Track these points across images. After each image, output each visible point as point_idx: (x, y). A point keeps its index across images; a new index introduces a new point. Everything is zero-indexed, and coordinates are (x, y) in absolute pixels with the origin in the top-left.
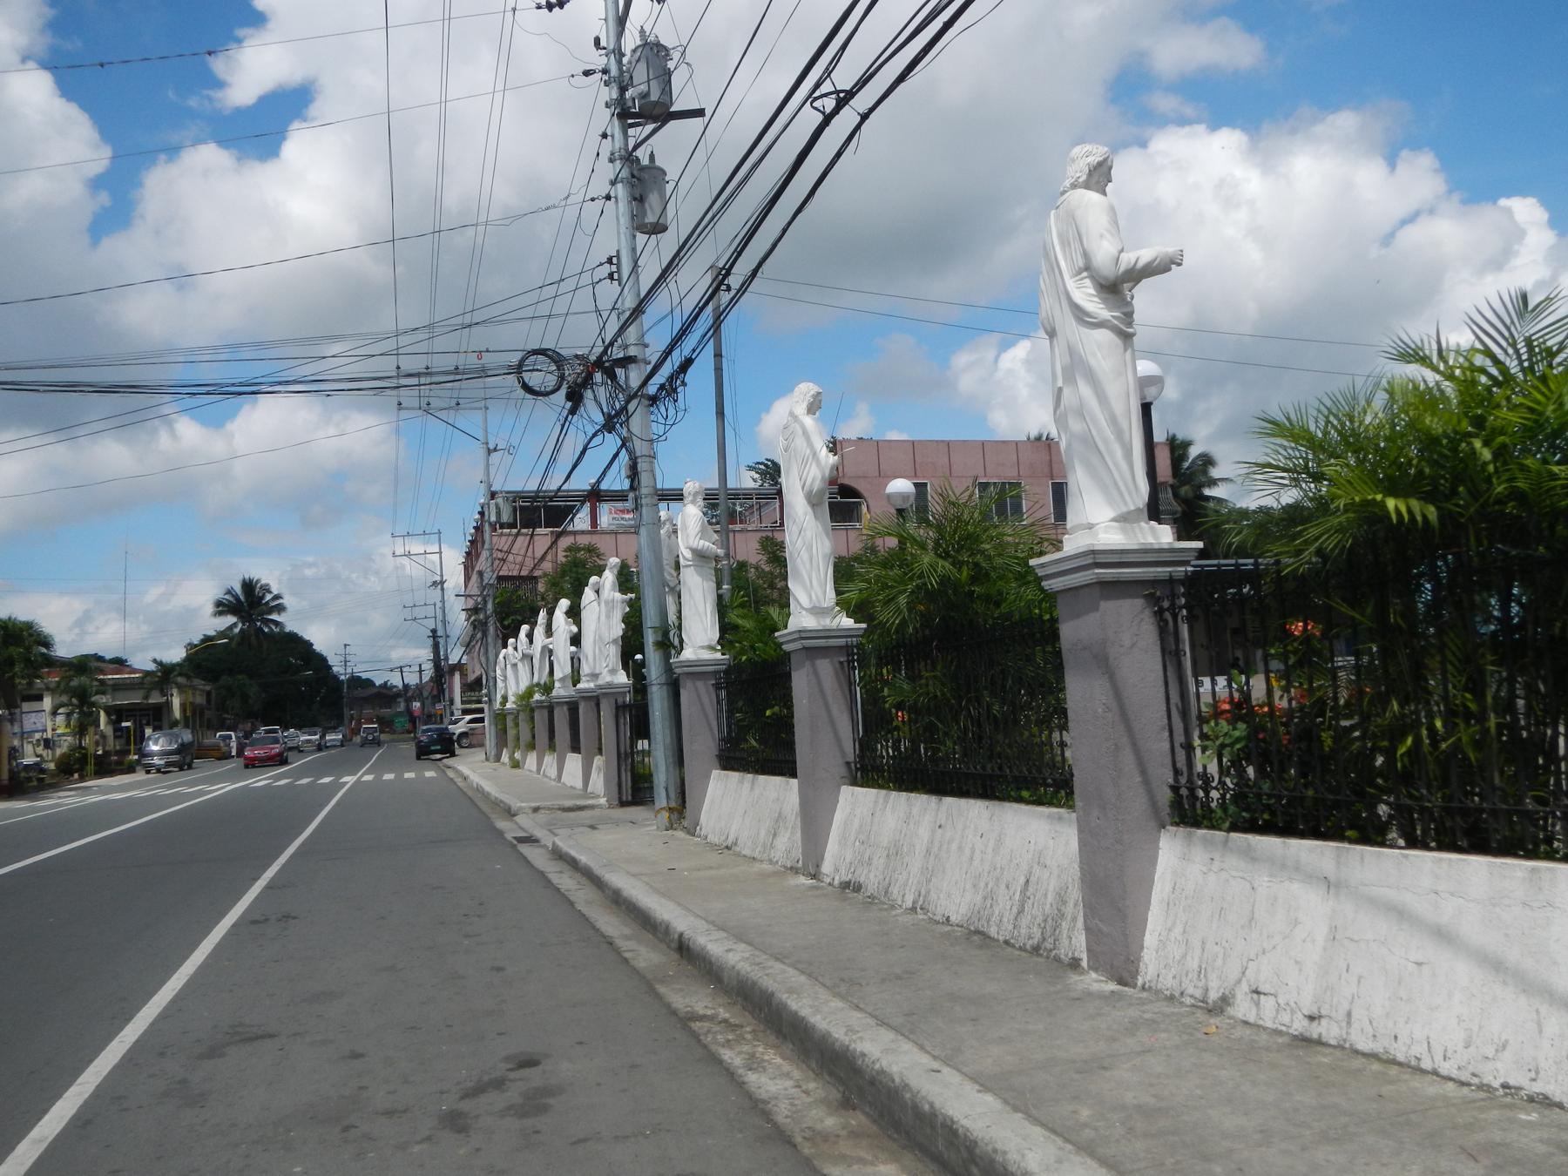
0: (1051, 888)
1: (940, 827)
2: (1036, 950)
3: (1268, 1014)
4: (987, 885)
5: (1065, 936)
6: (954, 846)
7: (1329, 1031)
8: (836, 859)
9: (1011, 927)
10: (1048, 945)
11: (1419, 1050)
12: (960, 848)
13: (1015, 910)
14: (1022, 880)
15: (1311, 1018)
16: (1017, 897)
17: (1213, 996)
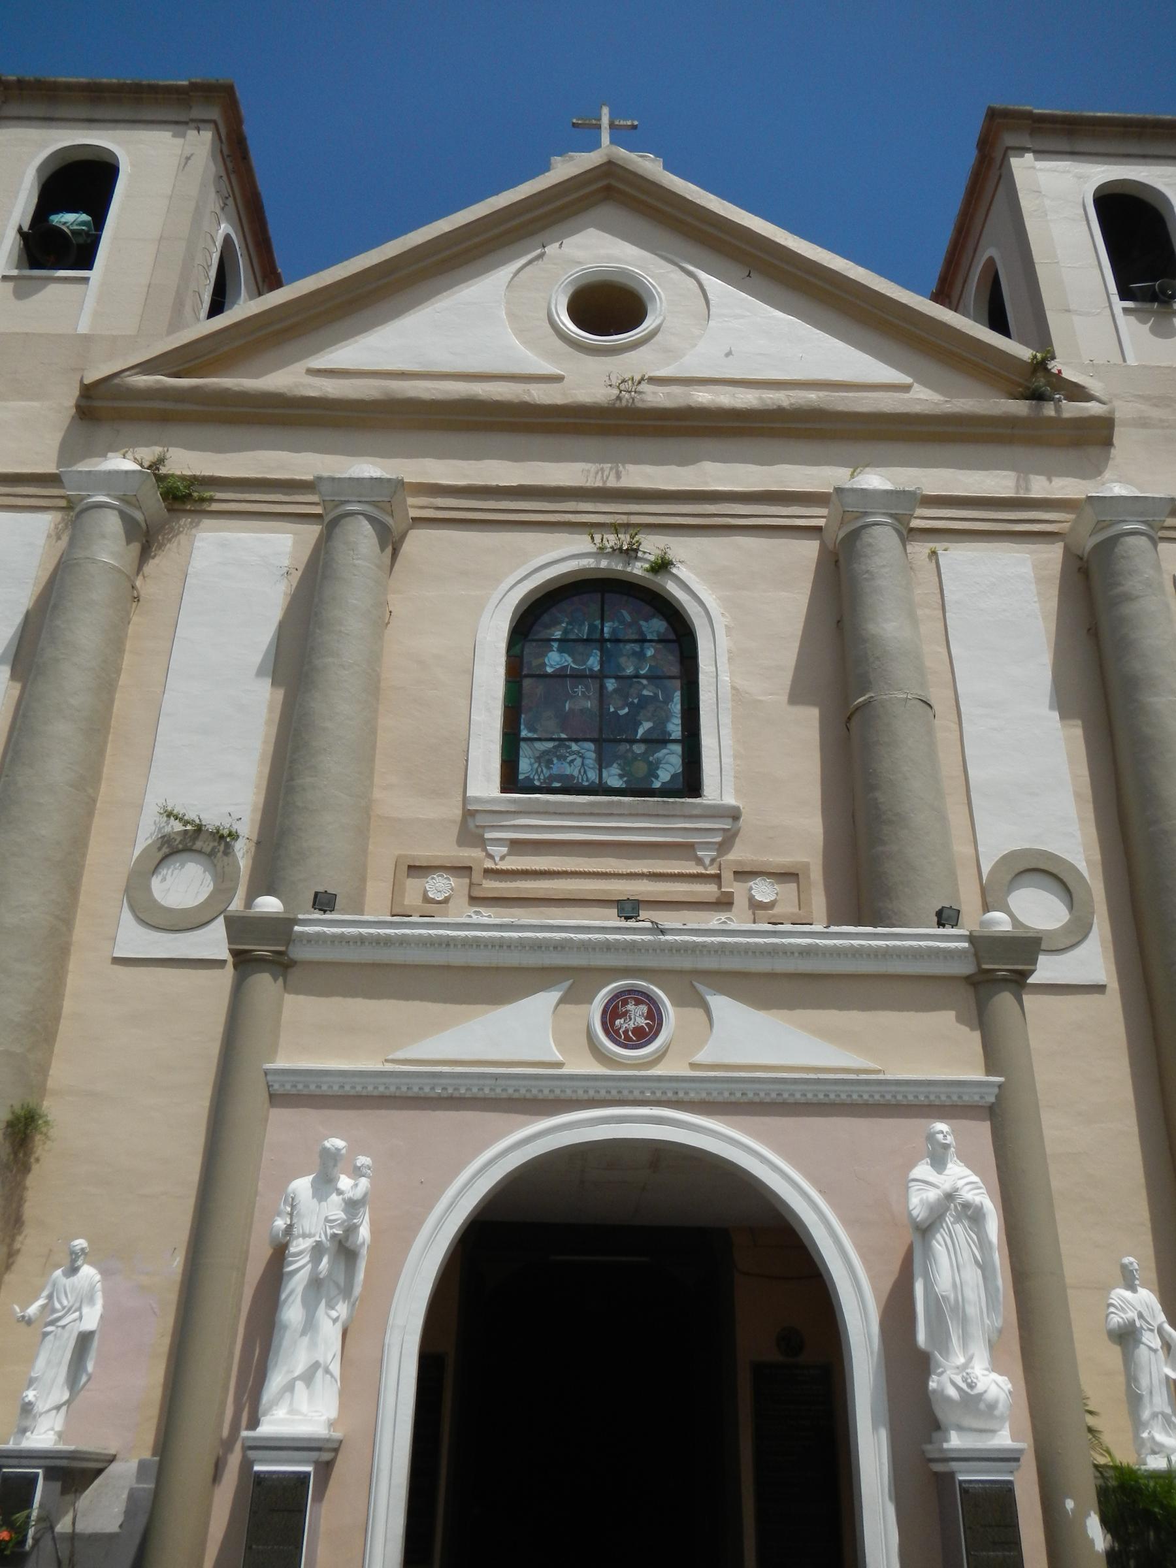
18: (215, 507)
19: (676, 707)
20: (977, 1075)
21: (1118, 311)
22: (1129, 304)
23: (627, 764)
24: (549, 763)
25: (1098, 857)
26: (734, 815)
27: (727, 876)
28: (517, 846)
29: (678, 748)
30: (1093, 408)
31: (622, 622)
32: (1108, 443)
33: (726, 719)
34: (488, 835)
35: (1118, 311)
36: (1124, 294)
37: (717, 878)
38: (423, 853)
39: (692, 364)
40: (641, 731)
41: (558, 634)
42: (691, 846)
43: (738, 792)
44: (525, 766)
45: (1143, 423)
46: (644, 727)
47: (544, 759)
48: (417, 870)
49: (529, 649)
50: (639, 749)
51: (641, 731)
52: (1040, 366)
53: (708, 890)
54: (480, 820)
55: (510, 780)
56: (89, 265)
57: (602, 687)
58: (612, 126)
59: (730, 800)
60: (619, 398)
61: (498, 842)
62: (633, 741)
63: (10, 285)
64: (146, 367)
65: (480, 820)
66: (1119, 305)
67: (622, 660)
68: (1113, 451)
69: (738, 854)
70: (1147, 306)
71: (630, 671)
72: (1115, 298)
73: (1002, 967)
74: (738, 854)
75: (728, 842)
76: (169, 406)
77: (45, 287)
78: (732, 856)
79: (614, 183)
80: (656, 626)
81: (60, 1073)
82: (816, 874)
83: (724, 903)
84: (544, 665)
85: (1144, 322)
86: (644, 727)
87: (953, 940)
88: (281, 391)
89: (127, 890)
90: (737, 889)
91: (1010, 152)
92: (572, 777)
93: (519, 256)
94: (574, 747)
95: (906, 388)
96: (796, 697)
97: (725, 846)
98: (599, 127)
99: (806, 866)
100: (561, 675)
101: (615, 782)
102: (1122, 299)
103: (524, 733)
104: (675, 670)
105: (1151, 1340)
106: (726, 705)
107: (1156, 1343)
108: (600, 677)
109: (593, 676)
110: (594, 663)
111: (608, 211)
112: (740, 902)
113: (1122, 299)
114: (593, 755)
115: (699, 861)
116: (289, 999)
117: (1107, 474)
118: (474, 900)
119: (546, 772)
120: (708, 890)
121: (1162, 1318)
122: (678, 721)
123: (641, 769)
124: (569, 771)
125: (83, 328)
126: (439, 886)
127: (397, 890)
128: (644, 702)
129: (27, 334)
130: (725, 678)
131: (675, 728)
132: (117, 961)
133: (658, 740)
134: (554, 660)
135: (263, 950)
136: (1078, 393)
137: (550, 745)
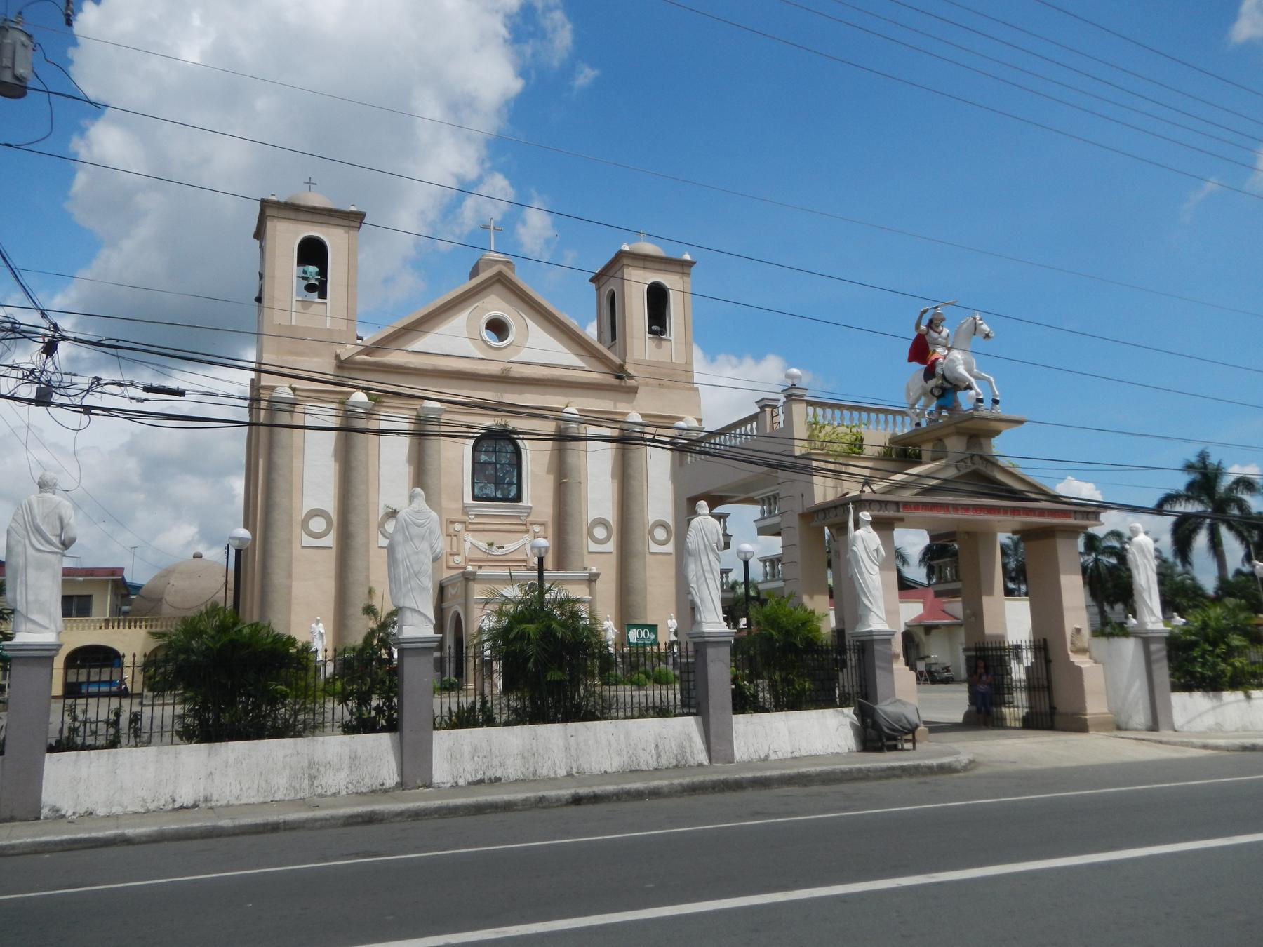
0: (673, 745)
1: (572, 736)
2: (676, 766)
3: (780, 756)
4: (628, 752)
5: (690, 757)
6: (591, 742)
7: (797, 754)
8: (441, 772)
9: (655, 763)
10: (683, 762)
11: (815, 752)
12: (597, 742)
13: (655, 757)
14: (653, 746)
15: (792, 753)
16: (653, 751)
17: (762, 757)
18: (385, 404)
19: (515, 473)
20: (588, 597)
21: (647, 338)
22: (651, 336)
23: (503, 490)
24: (482, 491)
25: (616, 519)
26: (530, 508)
27: (528, 524)
28: (476, 516)
29: (516, 486)
30: (632, 383)
31: (501, 446)
32: (636, 392)
33: (529, 480)
34: (470, 513)
35: (647, 338)
36: (650, 331)
37: (525, 525)
38: (454, 518)
39: (524, 355)
40: (506, 481)
41: (484, 450)
42: (519, 516)
43: (532, 501)
44: (476, 490)
45: (647, 385)
46: (508, 479)
47: (481, 489)
48: (453, 522)
49: (476, 453)
50: (506, 486)
51: (506, 481)
52: (621, 367)
53: (523, 528)
54: (468, 509)
55: (475, 498)
56: (326, 298)
57: (496, 467)
58: (494, 228)
59: (530, 505)
60: (503, 373)
61: (472, 515)
62: (504, 484)
63: (300, 303)
64: (359, 353)
65: (468, 509)
66: (648, 335)
67: (501, 459)
68: (637, 395)
69: (531, 519)
70: (655, 336)
71: (503, 462)
72: (647, 333)
73: (593, 578)
74: (531, 519)
75: (529, 514)
76: (367, 367)
77: (310, 306)
78: (528, 519)
79: (502, 279)
80: (510, 448)
81: (372, 578)
82: (550, 524)
83: (527, 532)
84: (480, 460)
85: (653, 342)
86: (508, 479)
87: (586, 573)
88: (403, 364)
89: (379, 527)
90: (529, 527)
91: (625, 267)
92: (488, 494)
93: (470, 306)
94: (489, 485)
95: (582, 369)
96: (548, 472)
97: (527, 516)
98: (490, 229)
99: (547, 522)
100: (485, 463)
101: (499, 495)
102: (649, 333)
103: (476, 481)
104: (515, 462)
105: (611, 631)
106: (529, 476)
107: (611, 631)
108: (496, 463)
109: (493, 463)
110: (493, 459)
111: (498, 287)
112: (531, 531)
113: (649, 333)
114: (493, 488)
115: (521, 520)
116: (475, 585)
117: (634, 403)
118: (467, 531)
119: (482, 493)
120: (523, 528)
121: (613, 627)
122: (516, 478)
123: (506, 492)
124: (488, 492)
125: (328, 327)
126: (458, 527)
127: (447, 527)
128: (507, 472)
129: (310, 328)
130: (529, 468)
131: (515, 480)
132: (379, 547)
133: (510, 484)
134: (483, 458)
135: (472, 577)
136: (631, 377)
137: (482, 484)
